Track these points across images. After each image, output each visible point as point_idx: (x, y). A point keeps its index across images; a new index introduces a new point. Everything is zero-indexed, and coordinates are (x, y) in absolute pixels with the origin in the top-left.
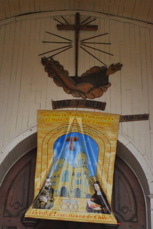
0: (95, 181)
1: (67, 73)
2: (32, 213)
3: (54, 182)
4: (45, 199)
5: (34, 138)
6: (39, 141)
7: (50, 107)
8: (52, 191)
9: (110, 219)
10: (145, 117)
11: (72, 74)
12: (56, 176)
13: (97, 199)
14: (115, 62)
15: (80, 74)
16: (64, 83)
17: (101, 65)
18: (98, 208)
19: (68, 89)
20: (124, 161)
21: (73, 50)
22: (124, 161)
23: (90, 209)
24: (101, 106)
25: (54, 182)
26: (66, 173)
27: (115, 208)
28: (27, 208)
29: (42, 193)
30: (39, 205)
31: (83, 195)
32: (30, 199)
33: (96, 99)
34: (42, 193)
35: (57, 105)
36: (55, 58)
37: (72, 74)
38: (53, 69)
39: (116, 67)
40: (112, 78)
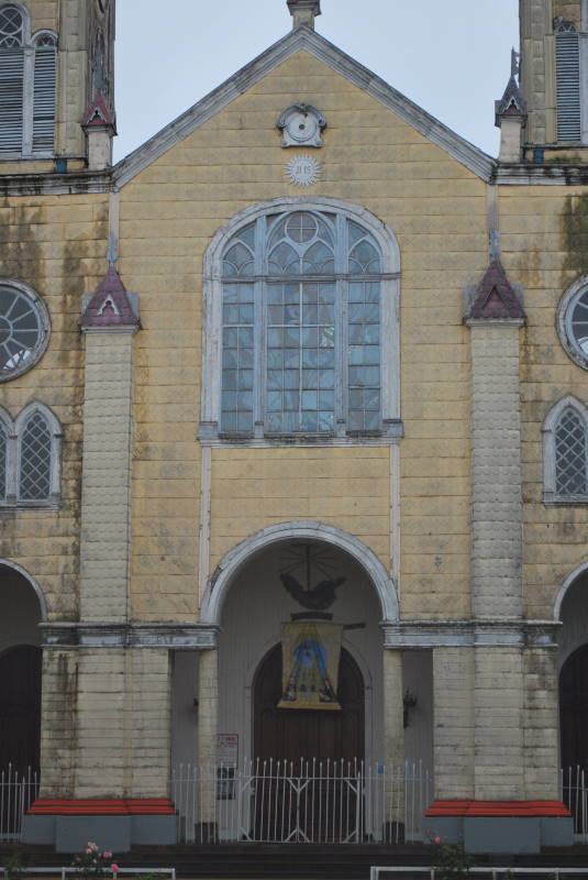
0: (326, 678)
2: (282, 704)
3: (296, 681)
4: (291, 694)
5: (278, 647)
6: (284, 648)
7: (289, 619)
8: (295, 688)
9: (336, 706)
10: (362, 625)
12: (297, 676)
13: (328, 692)
15: (312, 587)
16: (324, 44)
18: (328, 698)
20: (346, 661)
22: (346, 661)
23: (322, 700)
24: (329, 617)
25: (296, 681)
26: (304, 675)
27: (339, 699)
28: (277, 702)
29: (288, 689)
30: (286, 698)
31: (317, 689)
32: (278, 694)
33: (329, 611)
34: (288, 689)
35: (295, 617)
37: (305, 588)
38: (289, 584)
39: (341, 581)
40: (339, 592)
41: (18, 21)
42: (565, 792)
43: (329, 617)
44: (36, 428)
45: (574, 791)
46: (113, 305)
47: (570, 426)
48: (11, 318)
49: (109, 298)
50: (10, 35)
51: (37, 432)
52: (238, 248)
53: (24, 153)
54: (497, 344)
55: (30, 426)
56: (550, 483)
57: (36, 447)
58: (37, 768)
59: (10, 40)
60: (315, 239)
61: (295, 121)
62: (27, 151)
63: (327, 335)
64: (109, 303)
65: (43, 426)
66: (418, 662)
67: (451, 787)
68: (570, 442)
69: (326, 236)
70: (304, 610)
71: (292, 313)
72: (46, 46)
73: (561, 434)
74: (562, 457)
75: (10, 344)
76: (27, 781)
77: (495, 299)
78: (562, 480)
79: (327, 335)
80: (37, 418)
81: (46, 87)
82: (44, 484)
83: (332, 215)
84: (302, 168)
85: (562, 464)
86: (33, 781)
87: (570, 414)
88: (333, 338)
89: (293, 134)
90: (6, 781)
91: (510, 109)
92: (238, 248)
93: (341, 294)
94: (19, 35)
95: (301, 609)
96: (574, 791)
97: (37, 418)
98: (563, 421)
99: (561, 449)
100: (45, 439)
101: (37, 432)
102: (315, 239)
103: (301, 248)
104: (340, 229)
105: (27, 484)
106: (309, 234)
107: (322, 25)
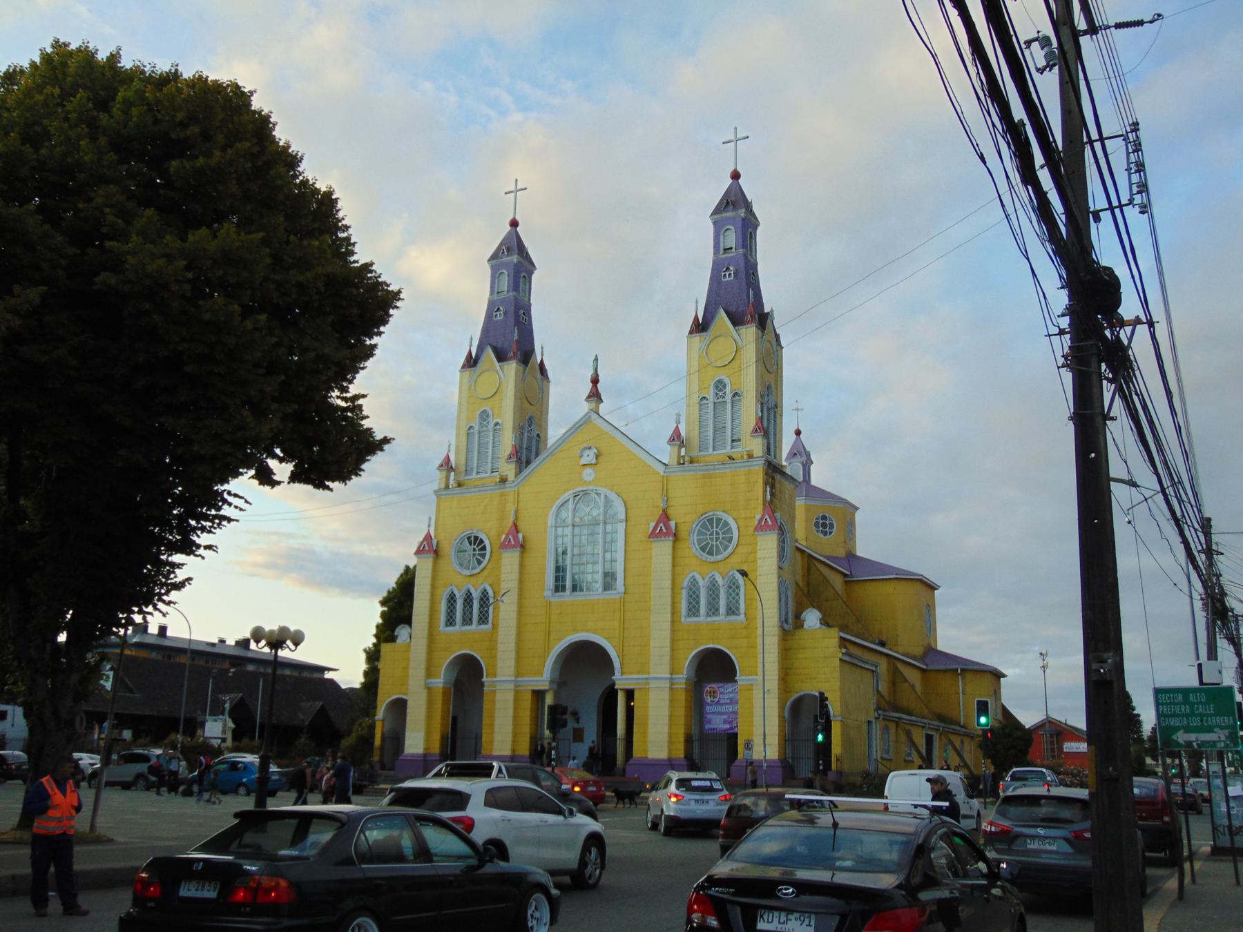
44: (485, 593)
54: (663, 549)
61: (587, 452)
66: (630, 694)
77: (665, 527)
84: (588, 474)
89: (584, 460)
91: (676, 438)
93: (600, 529)
104: (601, 502)
107: (603, 408)
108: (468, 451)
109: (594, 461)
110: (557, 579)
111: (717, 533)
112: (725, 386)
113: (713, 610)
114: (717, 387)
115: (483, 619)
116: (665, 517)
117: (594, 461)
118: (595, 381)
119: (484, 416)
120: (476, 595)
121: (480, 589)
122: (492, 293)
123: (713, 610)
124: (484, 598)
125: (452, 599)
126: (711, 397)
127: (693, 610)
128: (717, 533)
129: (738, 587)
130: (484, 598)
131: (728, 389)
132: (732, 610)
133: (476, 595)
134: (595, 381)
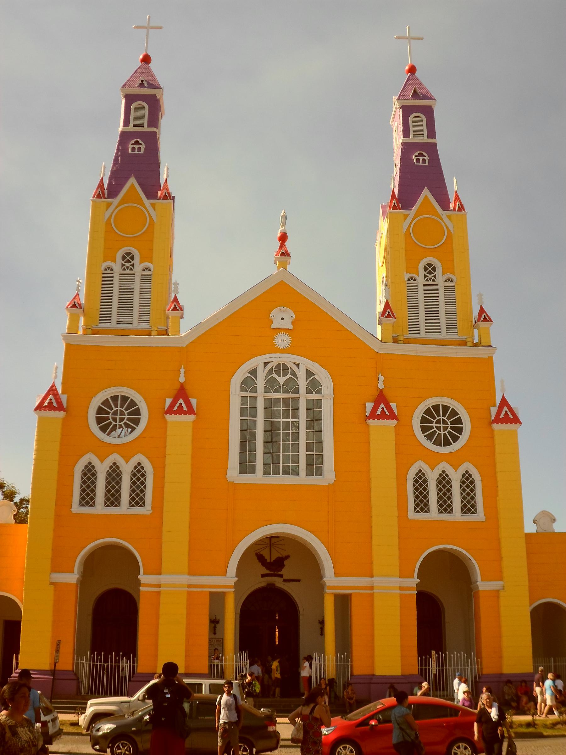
1: (266, 560)
10: (299, 581)
11: (268, 561)
14: (287, 554)
15: (272, 561)
17: (281, 556)
19: (267, 568)
21: (268, 548)
24: (281, 576)
33: (279, 573)
35: (263, 576)
36: (262, 553)
37: (268, 561)
38: (261, 558)
39: (287, 557)
40: (286, 562)
41: (133, 258)
42: (422, 670)
43: (281, 576)
45: (426, 669)
46: (184, 405)
47: (420, 478)
48: (126, 410)
49: (181, 401)
50: (128, 265)
51: (139, 471)
52: (248, 378)
53: (133, 325)
55: (135, 467)
56: (411, 505)
57: (138, 479)
58: (135, 655)
59: (128, 268)
60: (289, 376)
62: (135, 322)
63: (295, 426)
64: (181, 404)
65: (143, 468)
66: (343, 602)
67: (360, 668)
68: (421, 485)
69: (294, 374)
70: (268, 572)
71: (277, 415)
72: (147, 272)
73: (416, 481)
74: (417, 493)
75: (125, 423)
76: (130, 663)
78: (417, 505)
79: (295, 426)
80: (139, 464)
81: (146, 292)
82: (142, 499)
83: (297, 365)
85: (417, 497)
86: (133, 662)
87: (420, 471)
88: (298, 427)
90: (111, 662)
92: (248, 378)
94: (133, 265)
95: (268, 572)
96: (426, 669)
97: (139, 464)
98: (417, 474)
99: (417, 489)
100: (143, 475)
101: (139, 471)
102: (289, 376)
103: (282, 380)
105: (133, 499)
106: (285, 374)
108: (106, 295)
109: (290, 327)
110: (242, 458)
111: (444, 422)
112: (434, 269)
113: (445, 505)
114: (425, 269)
115: (137, 499)
116: (381, 398)
117: (290, 327)
118: (283, 238)
119: (128, 258)
120: (127, 470)
121: (134, 461)
122: (126, 123)
123: (445, 505)
124: (139, 474)
125: (89, 473)
126: (421, 280)
127: (422, 505)
128: (444, 422)
129: (472, 482)
130: (139, 474)
131: (439, 272)
132: (469, 507)
133: (127, 470)
134: (283, 238)
